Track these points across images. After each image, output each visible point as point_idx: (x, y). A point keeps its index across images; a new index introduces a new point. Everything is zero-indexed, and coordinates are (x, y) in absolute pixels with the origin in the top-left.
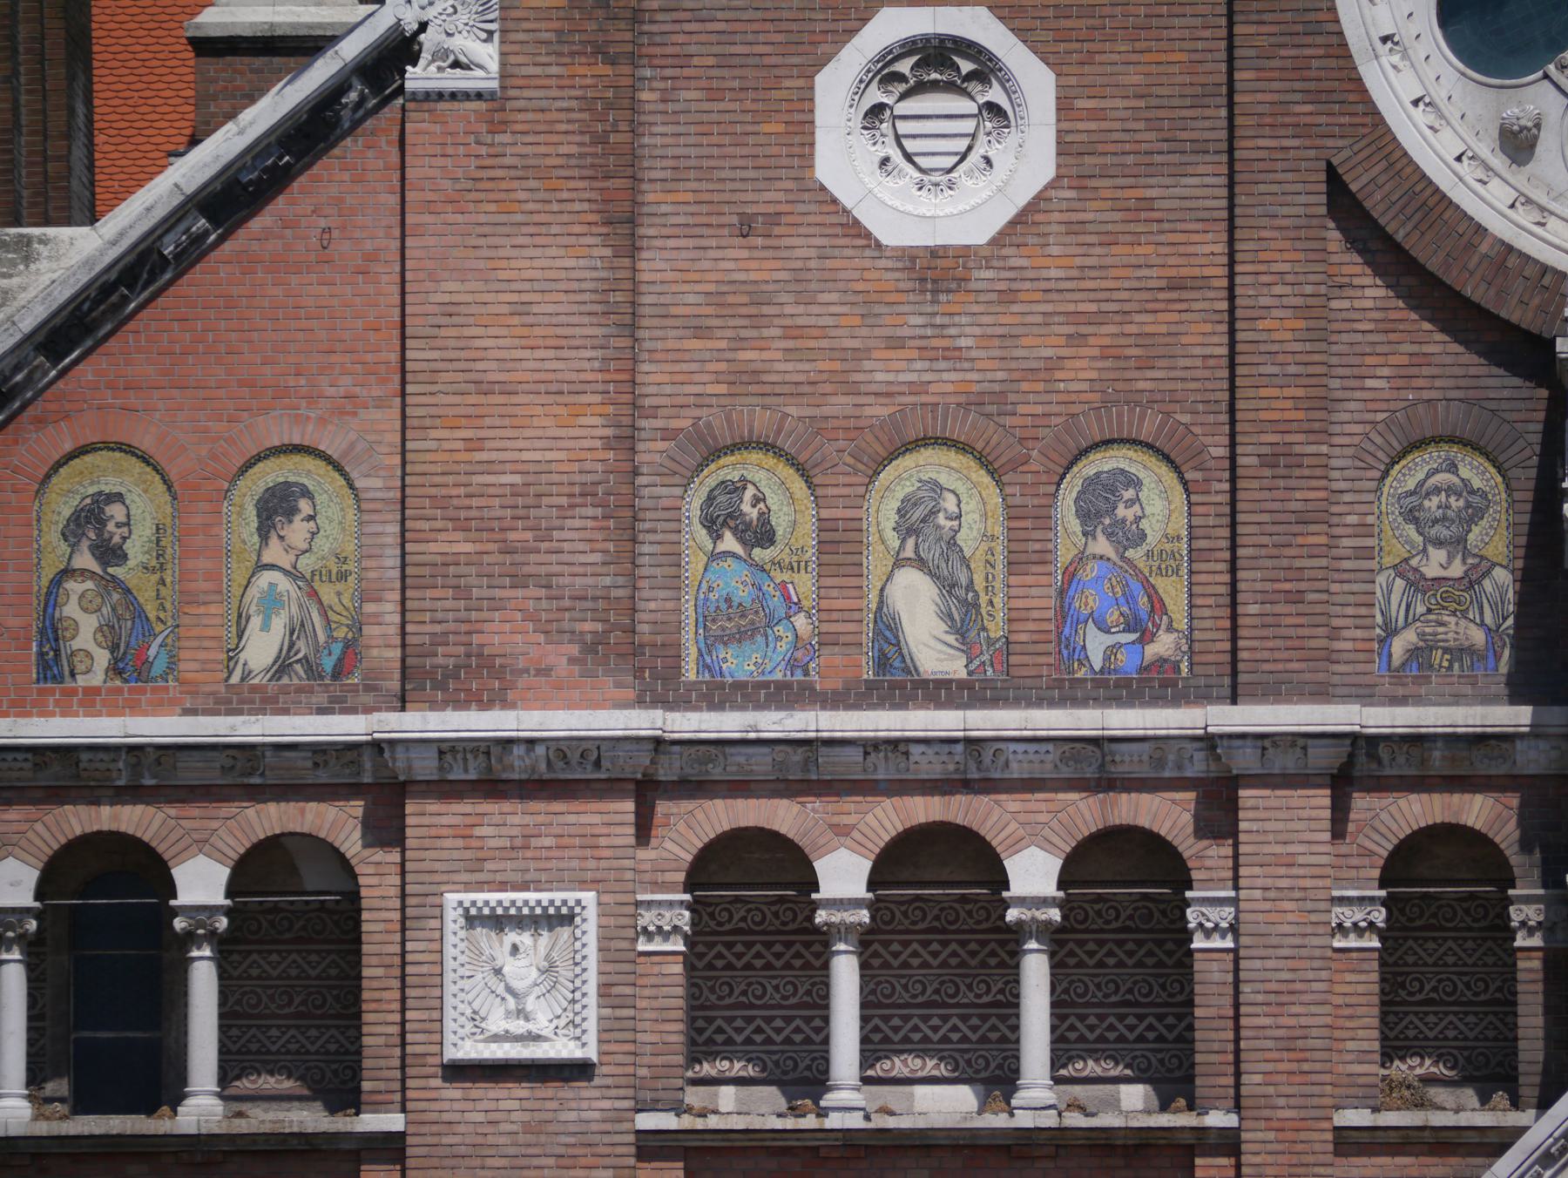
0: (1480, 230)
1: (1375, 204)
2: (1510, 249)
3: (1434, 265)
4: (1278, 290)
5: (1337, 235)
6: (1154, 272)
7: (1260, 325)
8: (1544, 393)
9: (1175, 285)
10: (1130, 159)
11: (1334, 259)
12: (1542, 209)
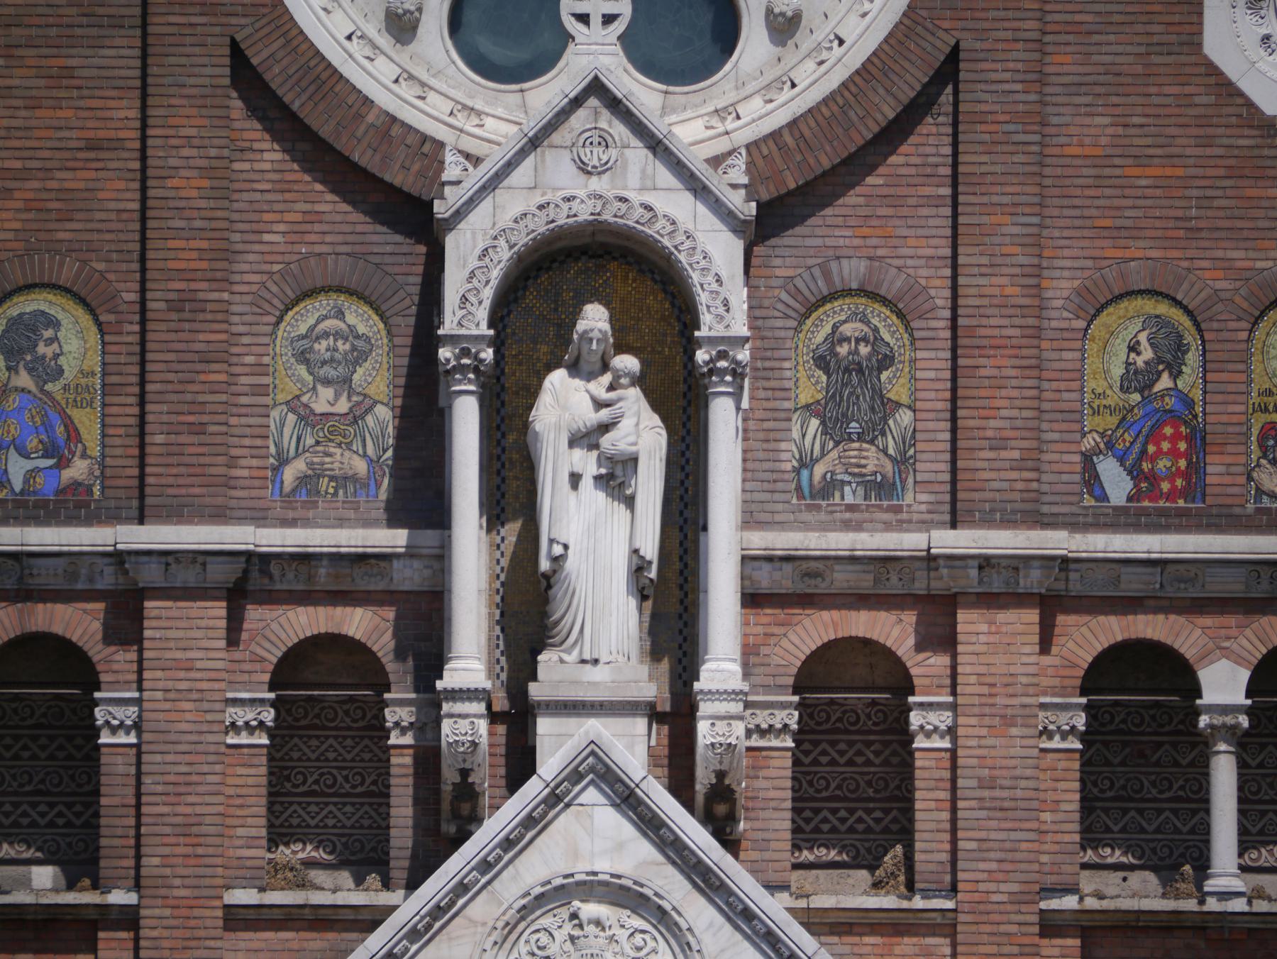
0: (367, 102)
1: (274, 77)
2: (394, 119)
3: (325, 131)
4: (186, 152)
5: (239, 103)
6: (74, 134)
7: (169, 183)
8: (422, 249)
9: (93, 146)
10: (53, 32)
11: (237, 125)
12: (423, 85)
